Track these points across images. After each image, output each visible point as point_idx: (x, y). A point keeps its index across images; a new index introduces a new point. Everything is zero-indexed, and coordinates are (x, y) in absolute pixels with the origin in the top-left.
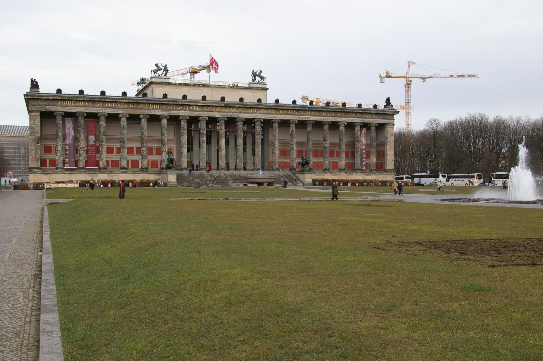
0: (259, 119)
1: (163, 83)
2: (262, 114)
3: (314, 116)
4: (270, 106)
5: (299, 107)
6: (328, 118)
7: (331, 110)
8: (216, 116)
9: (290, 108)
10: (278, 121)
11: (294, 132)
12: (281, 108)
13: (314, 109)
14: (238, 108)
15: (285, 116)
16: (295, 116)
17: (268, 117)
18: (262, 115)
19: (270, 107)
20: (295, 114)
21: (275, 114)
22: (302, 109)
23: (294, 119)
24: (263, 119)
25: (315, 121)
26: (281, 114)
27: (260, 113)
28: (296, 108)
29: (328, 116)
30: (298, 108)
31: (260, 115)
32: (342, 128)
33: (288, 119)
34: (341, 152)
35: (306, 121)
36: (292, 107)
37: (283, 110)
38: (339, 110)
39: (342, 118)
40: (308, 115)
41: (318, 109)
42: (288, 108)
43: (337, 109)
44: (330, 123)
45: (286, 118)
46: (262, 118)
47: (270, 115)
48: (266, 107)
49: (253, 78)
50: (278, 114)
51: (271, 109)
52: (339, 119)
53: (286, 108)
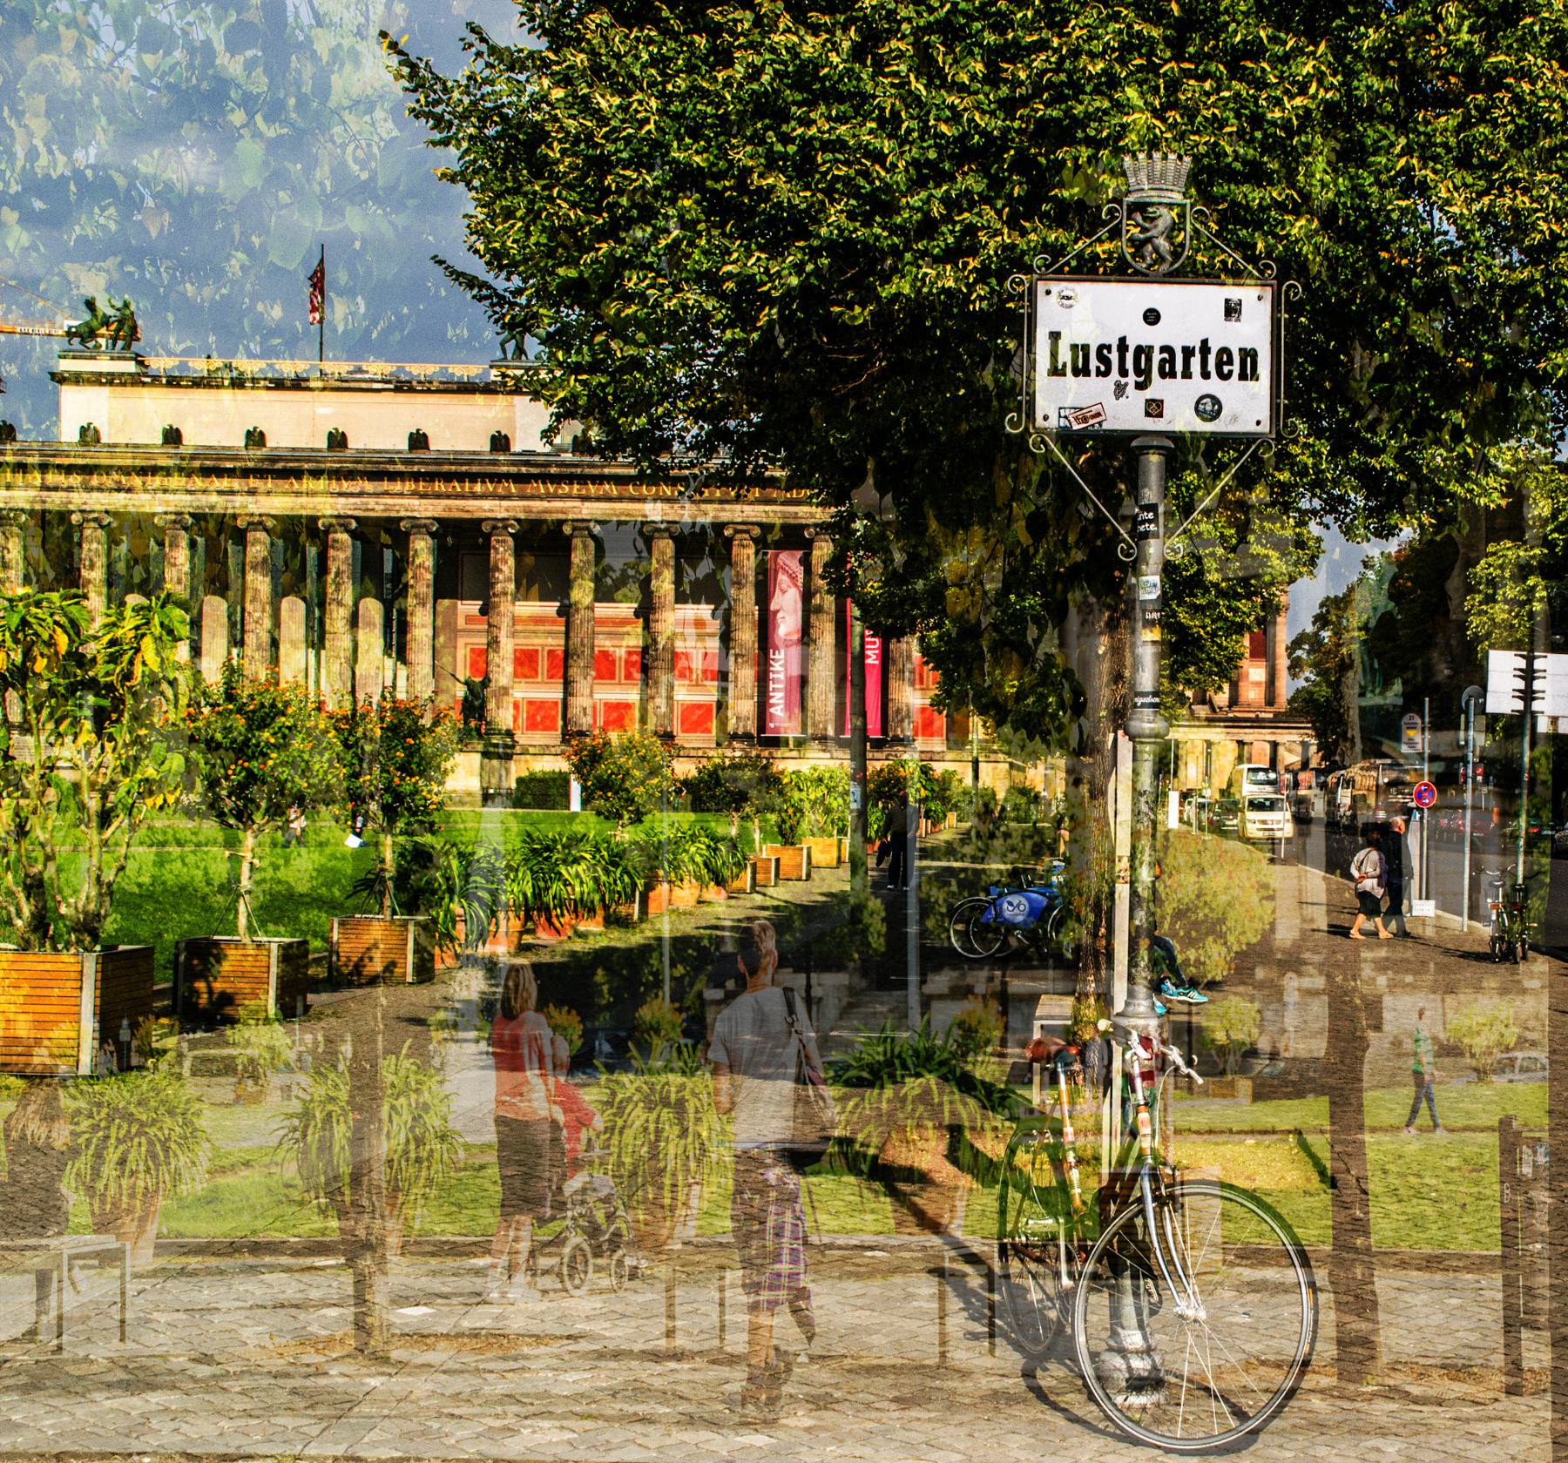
1: (100, 374)
2: (352, 495)
3: (598, 499)
5: (514, 463)
8: (147, 510)
9: (475, 469)
12: (432, 468)
14: (246, 473)
16: (505, 503)
17: (377, 507)
21: (414, 494)
22: (534, 470)
24: (357, 519)
26: (438, 496)
28: (504, 469)
30: (513, 470)
31: (342, 500)
33: (477, 515)
36: (480, 462)
37: (448, 477)
39: (738, 507)
40: (569, 497)
47: (390, 501)
49: (511, 346)
50: (424, 496)
51: (393, 476)
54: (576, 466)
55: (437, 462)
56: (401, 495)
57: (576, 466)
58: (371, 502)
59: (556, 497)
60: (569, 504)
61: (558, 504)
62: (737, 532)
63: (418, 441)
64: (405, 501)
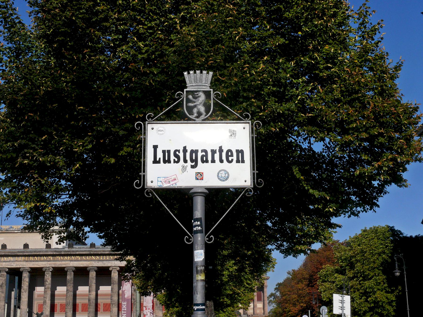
0: (3, 268)
2: (7, 262)
3: (75, 261)
4: (15, 252)
6: (93, 262)
7: (95, 253)
9: (41, 253)
10: (27, 270)
11: (47, 282)
13: (72, 253)
15: (36, 263)
16: (49, 262)
17: (14, 265)
18: (7, 263)
19: (16, 254)
20: (49, 260)
21: (24, 261)
22: (57, 253)
23: (48, 266)
24: (8, 268)
25: (75, 267)
26: (31, 261)
27: (4, 262)
28: (49, 253)
29: (94, 260)
30: (52, 253)
31: (4, 263)
32: (115, 275)
34: (112, 305)
35: (64, 267)
36: (43, 251)
38: (107, 253)
41: (77, 253)
42: (38, 253)
43: (103, 251)
44: (96, 269)
45: (37, 265)
46: (6, 267)
47: (18, 263)
48: (10, 254)
50: (27, 261)
51: (18, 256)
52: (109, 263)
53: (35, 253)
54: (69, 252)
55: (31, 252)
56: (21, 261)
57: (69, 252)
58: (12, 264)
59: (63, 260)
60: (67, 262)
61: (64, 262)
62: (113, 269)
63: (26, 246)
64: (22, 263)
